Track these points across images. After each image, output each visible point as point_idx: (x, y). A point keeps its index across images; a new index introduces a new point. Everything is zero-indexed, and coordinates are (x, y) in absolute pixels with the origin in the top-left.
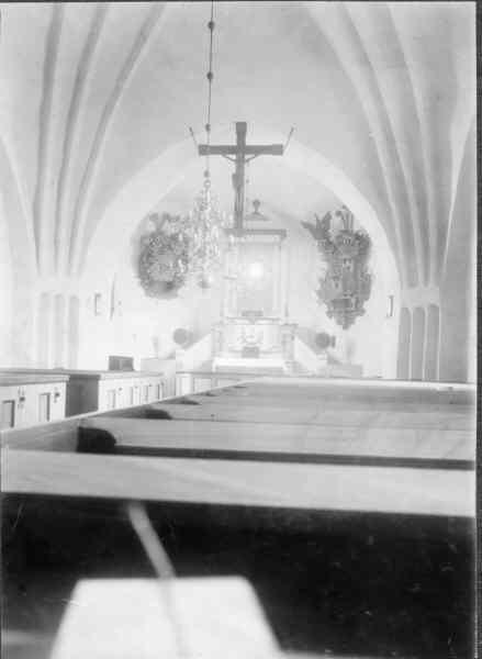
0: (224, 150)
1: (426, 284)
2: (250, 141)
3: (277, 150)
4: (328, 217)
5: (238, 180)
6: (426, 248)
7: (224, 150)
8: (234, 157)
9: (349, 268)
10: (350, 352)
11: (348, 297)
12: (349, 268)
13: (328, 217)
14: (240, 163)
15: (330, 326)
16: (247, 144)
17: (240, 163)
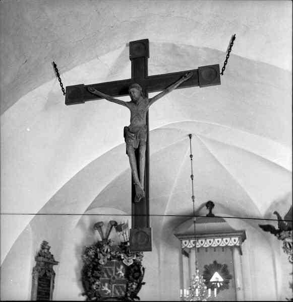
2: (154, 69)
8: (127, 99)
16: (150, 74)
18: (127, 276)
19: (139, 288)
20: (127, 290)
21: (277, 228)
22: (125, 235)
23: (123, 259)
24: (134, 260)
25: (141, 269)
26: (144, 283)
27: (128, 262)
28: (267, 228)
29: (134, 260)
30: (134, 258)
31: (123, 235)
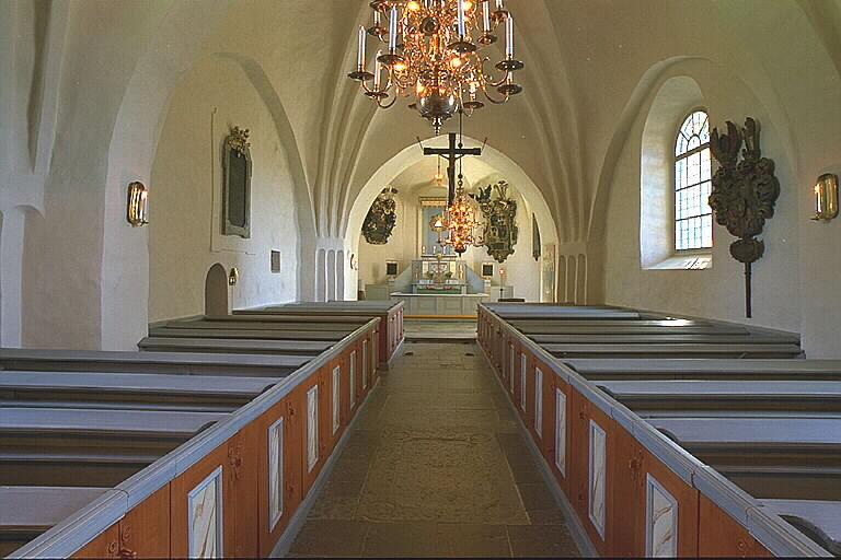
0: (440, 152)
1: (576, 239)
3: (476, 152)
4: (489, 188)
5: (451, 171)
6: (576, 217)
7: (440, 152)
8: (448, 156)
10: (503, 276)
11: (500, 241)
13: (489, 188)
14: (452, 161)
15: (489, 260)
17: (452, 161)
18: (386, 220)
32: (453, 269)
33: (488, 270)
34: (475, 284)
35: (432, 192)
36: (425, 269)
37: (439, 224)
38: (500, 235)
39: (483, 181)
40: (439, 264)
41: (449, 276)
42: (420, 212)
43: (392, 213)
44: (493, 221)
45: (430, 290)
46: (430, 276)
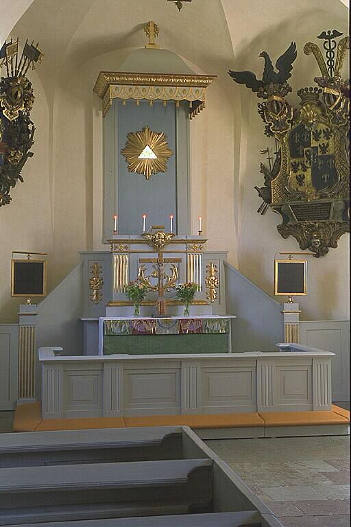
4: (290, 55)
9: (324, 148)
12: (324, 148)
13: (290, 55)
15: (289, 250)
19: (24, 160)
20: (6, 162)
21: (259, 78)
22: (10, 66)
23: (4, 108)
24: (19, 111)
25: (30, 127)
26: (31, 155)
27: (11, 114)
28: (243, 78)
29: (19, 111)
30: (21, 110)
31: (7, 65)
32: (196, 277)
33: (291, 278)
34: (255, 312)
35: (133, 61)
36: (121, 273)
37: (148, 154)
38: (317, 183)
39: (269, 36)
40: (159, 262)
41: (187, 295)
42: (98, 122)
43: (23, 120)
44: (298, 142)
45: (137, 337)
46: (136, 295)
